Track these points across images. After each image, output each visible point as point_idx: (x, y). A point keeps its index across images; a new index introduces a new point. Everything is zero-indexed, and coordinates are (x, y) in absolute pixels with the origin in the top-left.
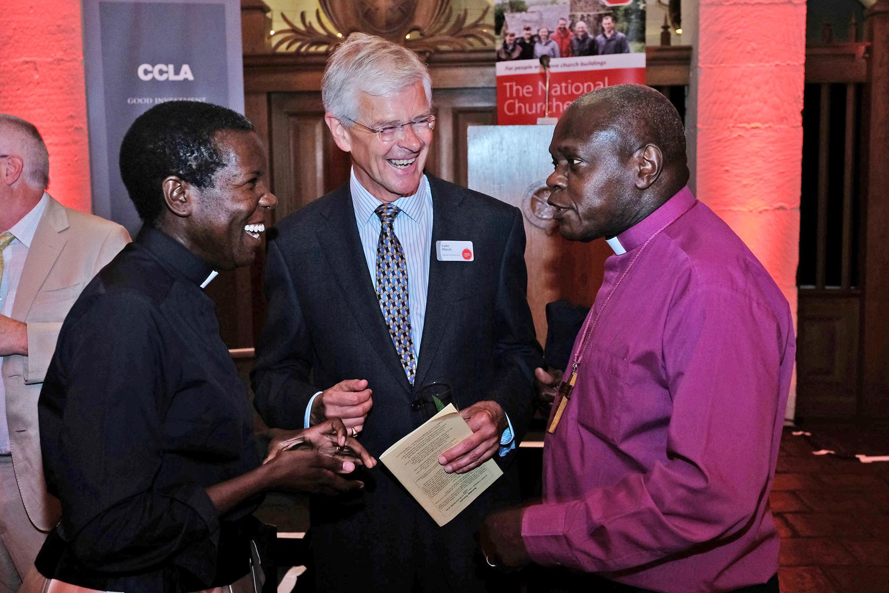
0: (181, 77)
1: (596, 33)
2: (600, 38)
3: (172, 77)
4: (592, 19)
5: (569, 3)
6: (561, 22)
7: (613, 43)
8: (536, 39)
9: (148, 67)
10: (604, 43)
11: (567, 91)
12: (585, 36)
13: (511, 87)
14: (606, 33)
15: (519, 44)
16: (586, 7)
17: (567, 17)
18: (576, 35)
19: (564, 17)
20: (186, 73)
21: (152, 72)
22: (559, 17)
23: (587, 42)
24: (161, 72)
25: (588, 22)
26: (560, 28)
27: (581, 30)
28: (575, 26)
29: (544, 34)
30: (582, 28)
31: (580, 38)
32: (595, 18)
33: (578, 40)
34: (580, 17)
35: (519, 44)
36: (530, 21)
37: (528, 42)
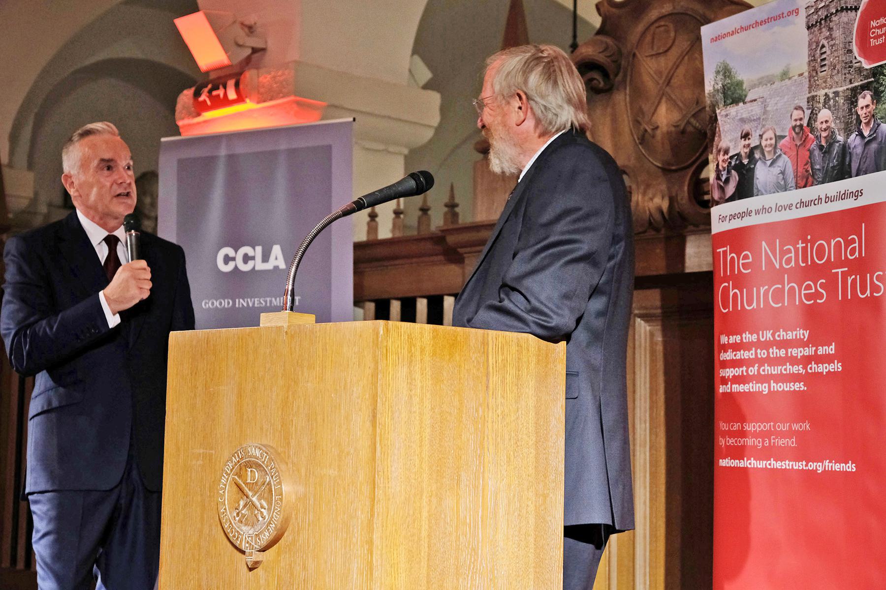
0: (269, 266)
1: (848, 132)
2: (854, 140)
3: (260, 266)
4: (841, 101)
5: (806, 74)
6: (797, 114)
7: (874, 146)
8: (757, 155)
9: (229, 251)
10: (859, 150)
11: (805, 260)
12: (831, 140)
13: (725, 252)
14: (863, 126)
15: (736, 168)
16: (832, 76)
17: (804, 104)
18: (818, 138)
19: (801, 105)
20: (276, 259)
21: (234, 259)
22: (793, 106)
23: (836, 148)
24: (246, 258)
25: (834, 109)
26: (794, 128)
27: (824, 126)
28: (815, 121)
29: (769, 142)
30: (826, 122)
31: (823, 143)
32: (847, 99)
33: (821, 147)
34: (822, 101)
35: (736, 168)
36: (750, 120)
37: (745, 161)
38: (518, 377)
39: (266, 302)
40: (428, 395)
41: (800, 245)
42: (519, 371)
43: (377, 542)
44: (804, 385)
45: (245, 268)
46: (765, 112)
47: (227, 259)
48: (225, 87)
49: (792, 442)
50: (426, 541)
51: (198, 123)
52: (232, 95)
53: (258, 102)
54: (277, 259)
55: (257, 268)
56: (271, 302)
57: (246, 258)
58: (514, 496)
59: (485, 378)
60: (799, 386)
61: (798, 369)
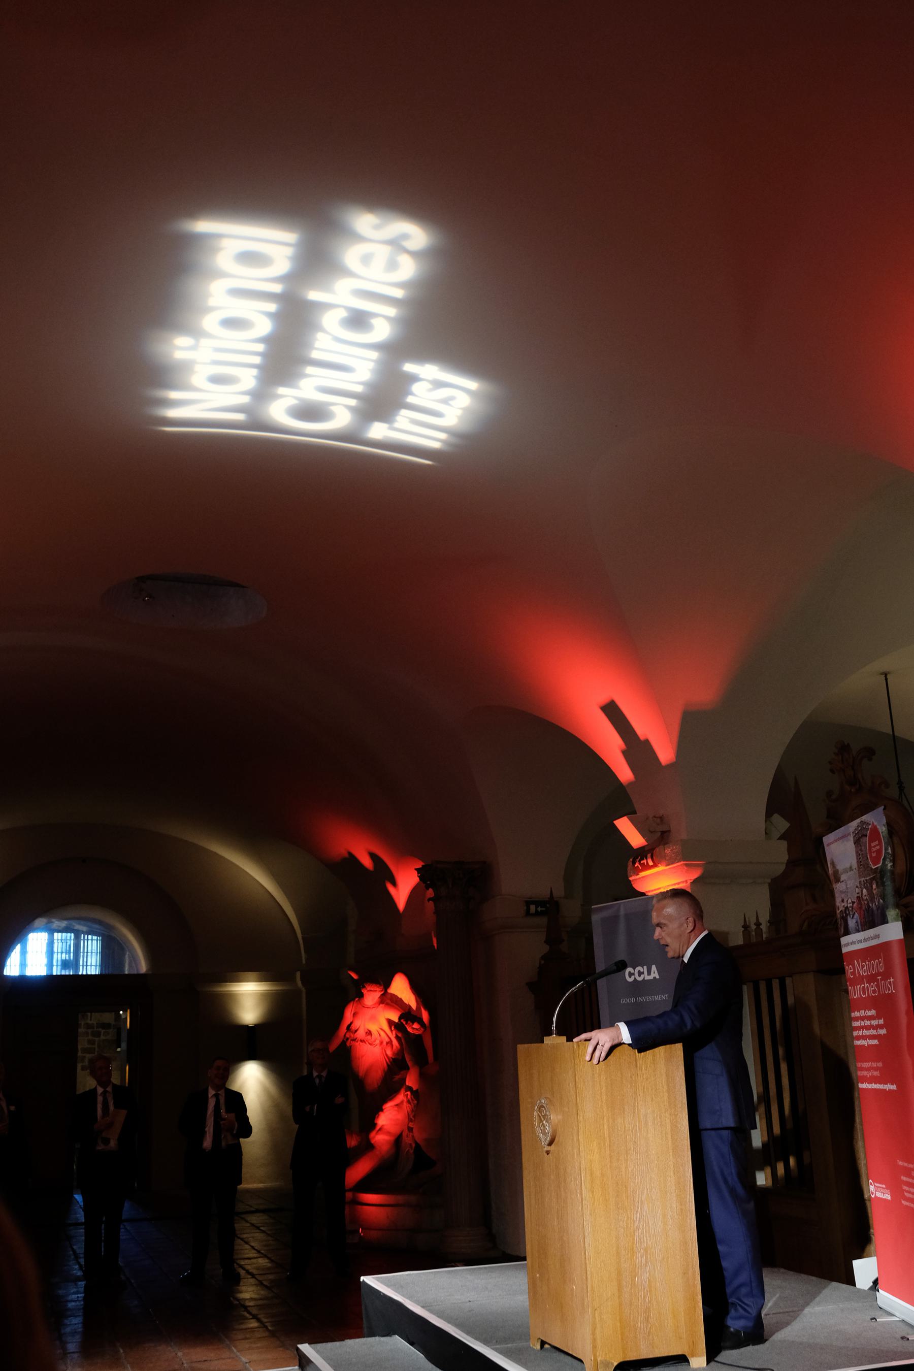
0: (651, 977)
3: (647, 978)
20: (654, 973)
24: (640, 973)
33: (866, 909)
38: (654, 1060)
39: (652, 998)
40: (603, 1073)
41: (867, 963)
42: (654, 1056)
43: (581, 1140)
44: (878, 1041)
45: (640, 979)
46: (847, 888)
47: (631, 974)
48: (647, 859)
49: (876, 1073)
50: (608, 1138)
51: (640, 878)
52: (651, 863)
53: (666, 866)
54: (655, 974)
55: (645, 979)
56: (654, 998)
57: (640, 973)
58: (657, 1115)
59: (635, 1063)
60: (875, 1042)
61: (873, 1032)
